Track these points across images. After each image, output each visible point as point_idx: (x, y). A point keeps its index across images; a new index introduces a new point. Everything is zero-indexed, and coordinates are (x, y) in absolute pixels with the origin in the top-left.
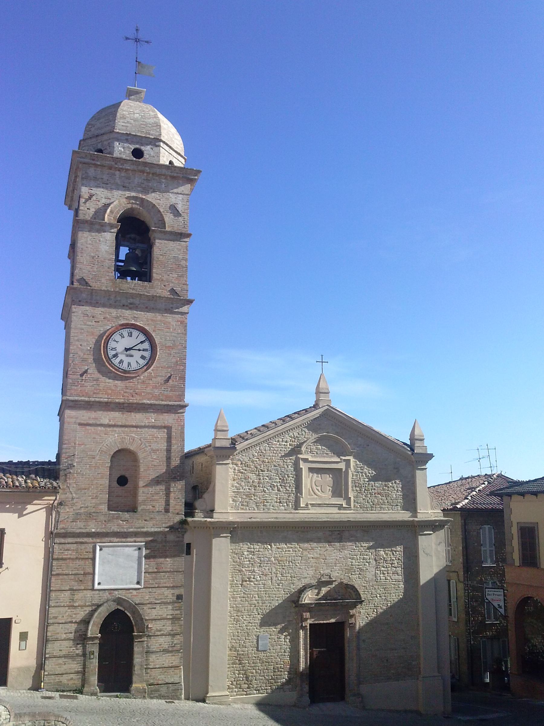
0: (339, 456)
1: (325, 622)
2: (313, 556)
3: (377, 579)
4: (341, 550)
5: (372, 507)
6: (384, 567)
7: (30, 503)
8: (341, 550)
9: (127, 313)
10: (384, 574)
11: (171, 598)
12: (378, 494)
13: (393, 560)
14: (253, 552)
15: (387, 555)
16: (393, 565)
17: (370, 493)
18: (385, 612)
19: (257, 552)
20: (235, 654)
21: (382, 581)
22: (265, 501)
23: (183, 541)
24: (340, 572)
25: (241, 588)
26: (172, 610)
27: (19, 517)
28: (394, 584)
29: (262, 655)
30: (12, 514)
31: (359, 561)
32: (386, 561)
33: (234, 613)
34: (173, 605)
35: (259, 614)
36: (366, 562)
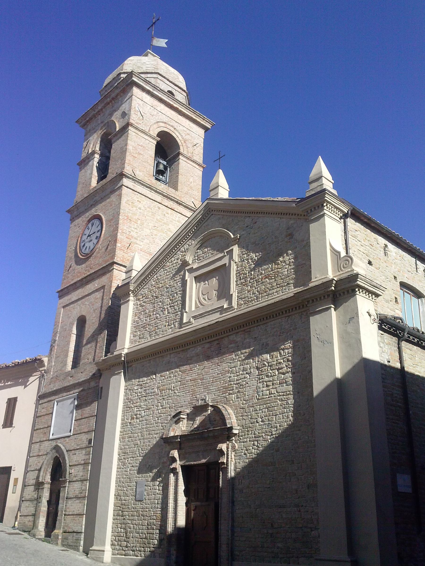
0: (222, 251)
1: (196, 463)
2: (191, 378)
3: (259, 395)
4: (220, 364)
5: (257, 298)
6: (267, 376)
7: (31, 376)
8: (220, 364)
9: (87, 214)
10: (267, 386)
11: (85, 444)
12: (266, 278)
13: (280, 363)
14: (142, 385)
15: (273, 358)
16: (281, 371)
17: (256, 280)
18: (270, 447)
19: (144, 385)
20: (119, 503)
21: (265, 397)
22: (157, 328)
23: (99, 385)
24: (217, 393)
25: (129, 426)
26: (85, 455)
27: (24, 388)
28: (282, 400)
29: (139, 505)
30: (21, 386)
31: (238, 374)
32: (271, 366)
33: (122, 456)
34: (86, 450)
35: (140, 456)
36: (247, 373)
